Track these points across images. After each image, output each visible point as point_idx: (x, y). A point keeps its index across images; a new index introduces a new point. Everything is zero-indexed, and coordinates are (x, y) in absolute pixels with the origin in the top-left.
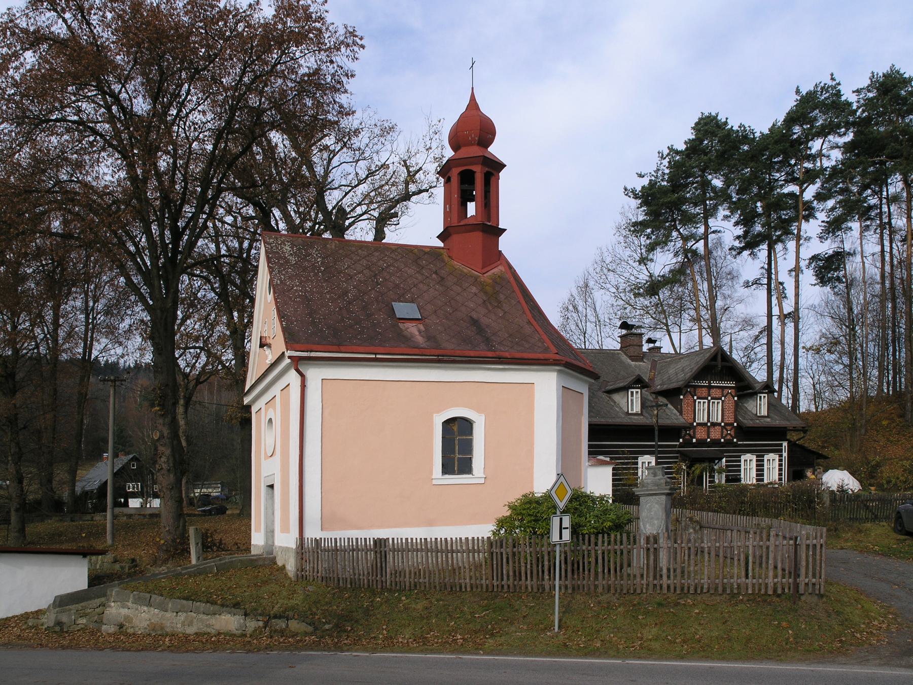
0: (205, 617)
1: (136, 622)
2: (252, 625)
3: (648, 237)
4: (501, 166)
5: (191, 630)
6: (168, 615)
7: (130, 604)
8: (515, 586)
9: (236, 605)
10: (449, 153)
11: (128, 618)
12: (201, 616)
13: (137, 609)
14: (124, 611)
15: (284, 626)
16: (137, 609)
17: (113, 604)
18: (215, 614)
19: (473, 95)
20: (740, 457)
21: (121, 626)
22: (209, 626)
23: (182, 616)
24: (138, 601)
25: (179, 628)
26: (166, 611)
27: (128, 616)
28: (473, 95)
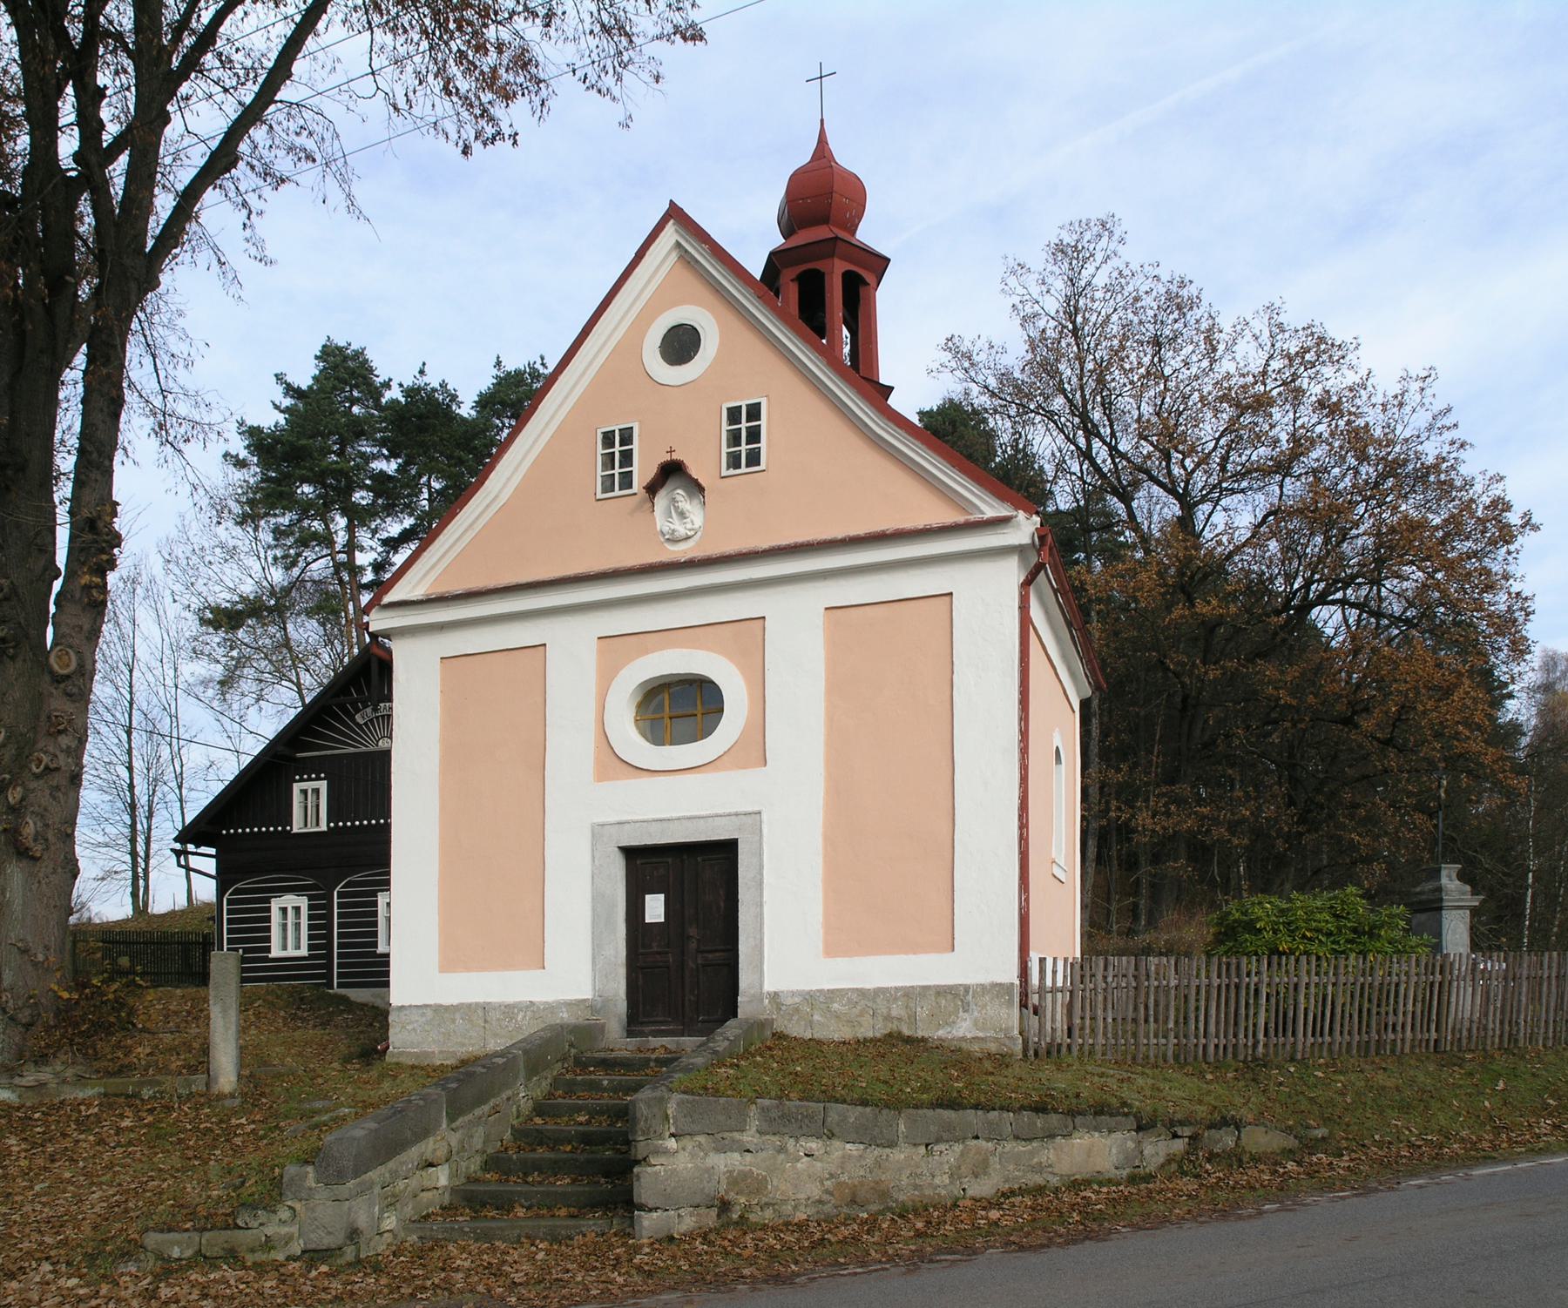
0: (1021, 1147)
1: (779, 1187)
2: (1157, 1150)
3: (1453, 548)
4: (344, 368)
5: (983, 1188)
6: (898, 1155)
7: (749, 1137)
8: (1165, 1037)
9: (1100, 1110)
10: (778, 240)
11: (737, 1180)
12: (1009, 1146)
13: (782, 1149)
14: (726, 1162)
15: (1231, 1144)
16: (782, 1149)
17: (672, 1144)
18: (1052, 1136)
19: (822, 140)
20: (375, 894)
21: (725, 1206)
22: (1039, 1169)
23: (950, 1154)
24: (781, 1124)
25: (941, 1184)
26: (892, 1144)
27: (745, 1175)
28: (822, 140)
